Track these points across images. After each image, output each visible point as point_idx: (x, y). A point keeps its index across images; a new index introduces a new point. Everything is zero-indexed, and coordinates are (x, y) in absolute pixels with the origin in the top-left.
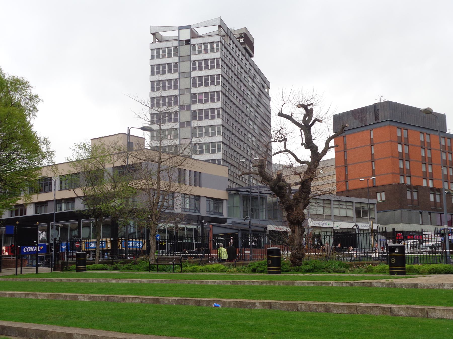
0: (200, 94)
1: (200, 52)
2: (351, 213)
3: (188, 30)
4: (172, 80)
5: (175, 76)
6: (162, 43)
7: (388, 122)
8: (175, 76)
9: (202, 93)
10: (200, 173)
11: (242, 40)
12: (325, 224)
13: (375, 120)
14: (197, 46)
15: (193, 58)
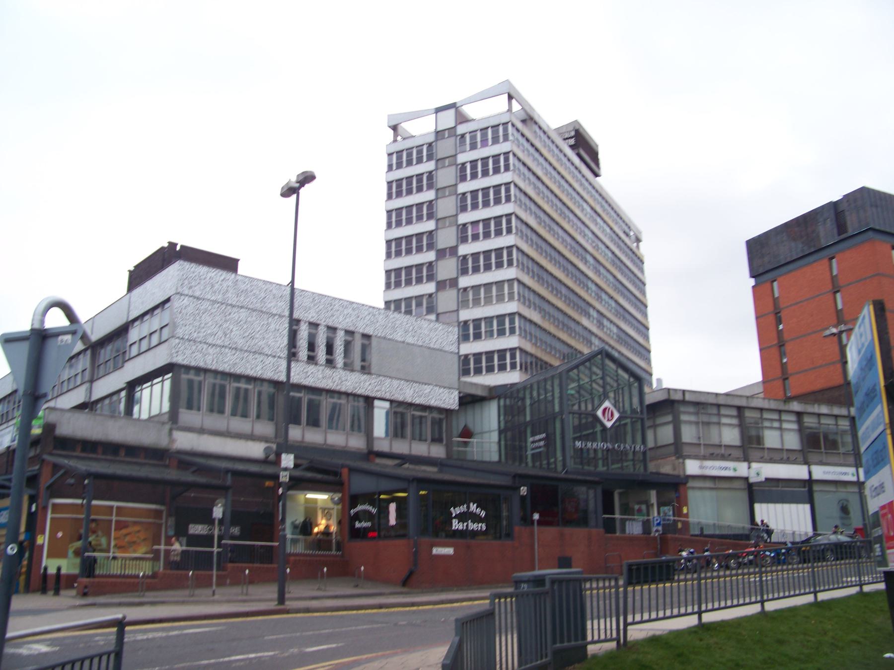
0: (475, 223)
1: (473, 147)
2: (792, 441)
3: (452, 112)
5: (428, 195)
6: (406, 141)
8: (428, 195)
10: (366, 336)
11: (572, 142)
12: (726, 468)
13: (839, 234)
15: (462, 158)
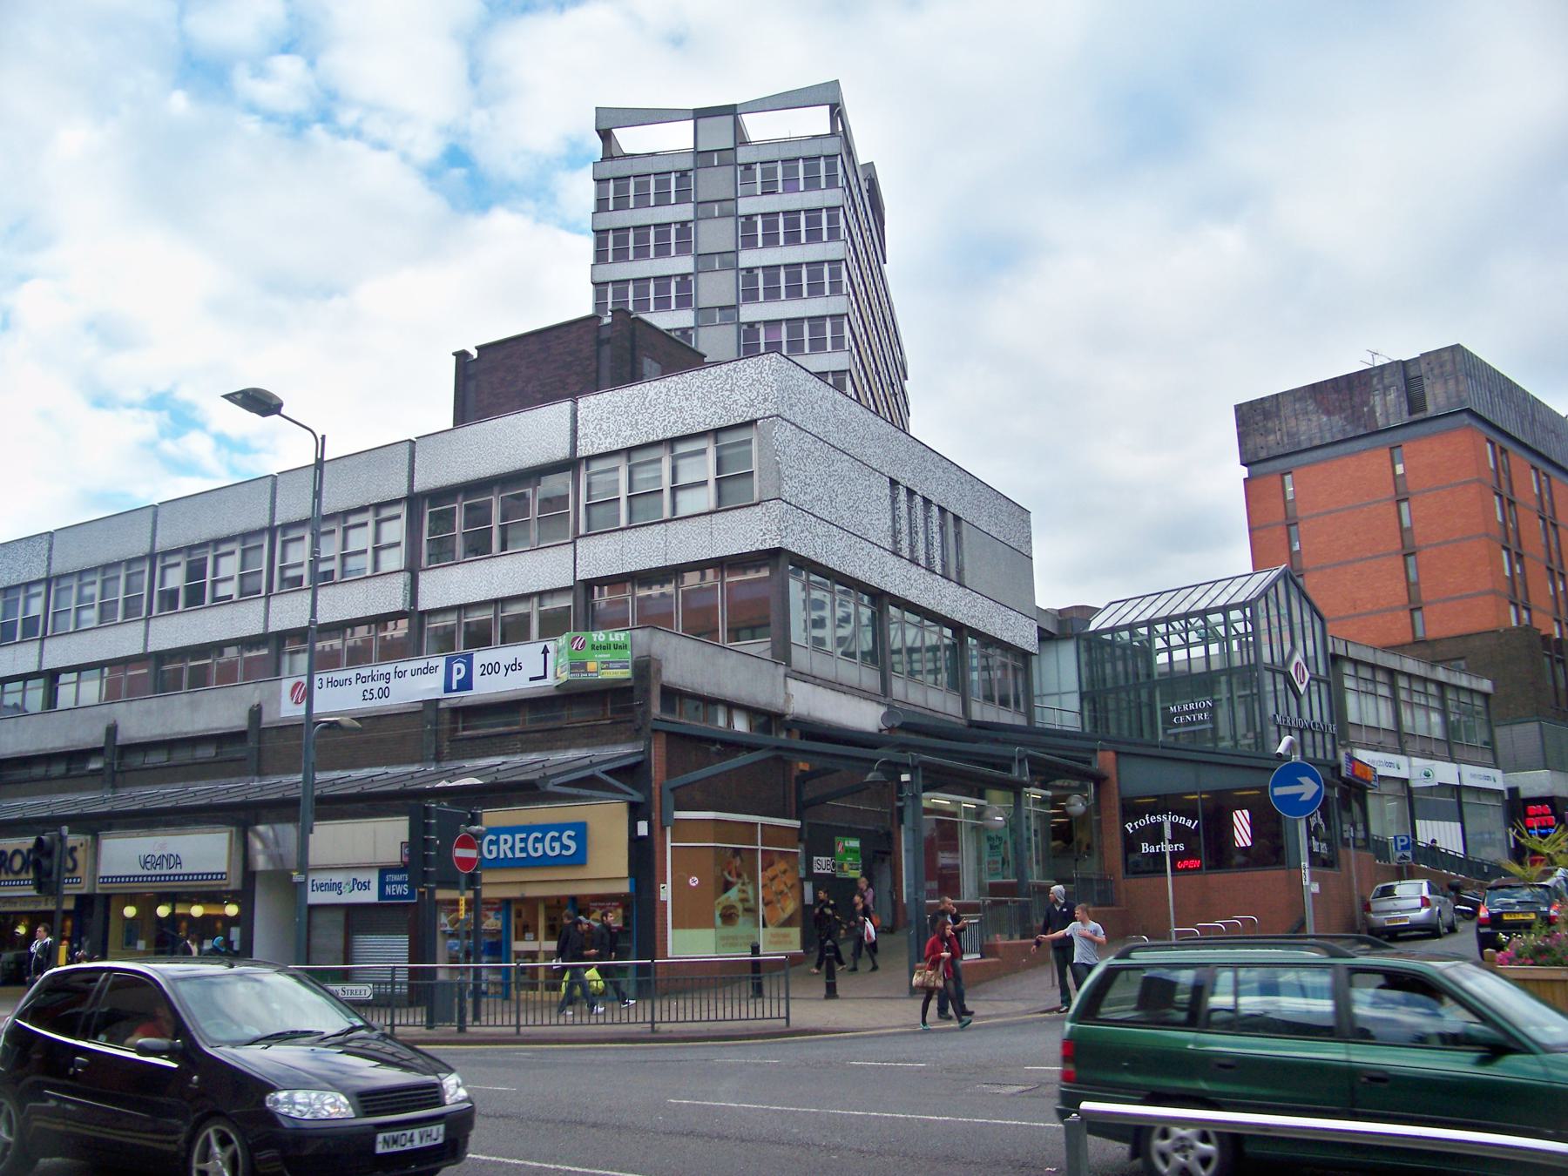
0: (772, 324)
1: (769, 189)
4: (669, 277)
7: (1465, 416)
9: (777, 323)
13: (1411, 413)
14: (758, 168)
15: (746, 206)
